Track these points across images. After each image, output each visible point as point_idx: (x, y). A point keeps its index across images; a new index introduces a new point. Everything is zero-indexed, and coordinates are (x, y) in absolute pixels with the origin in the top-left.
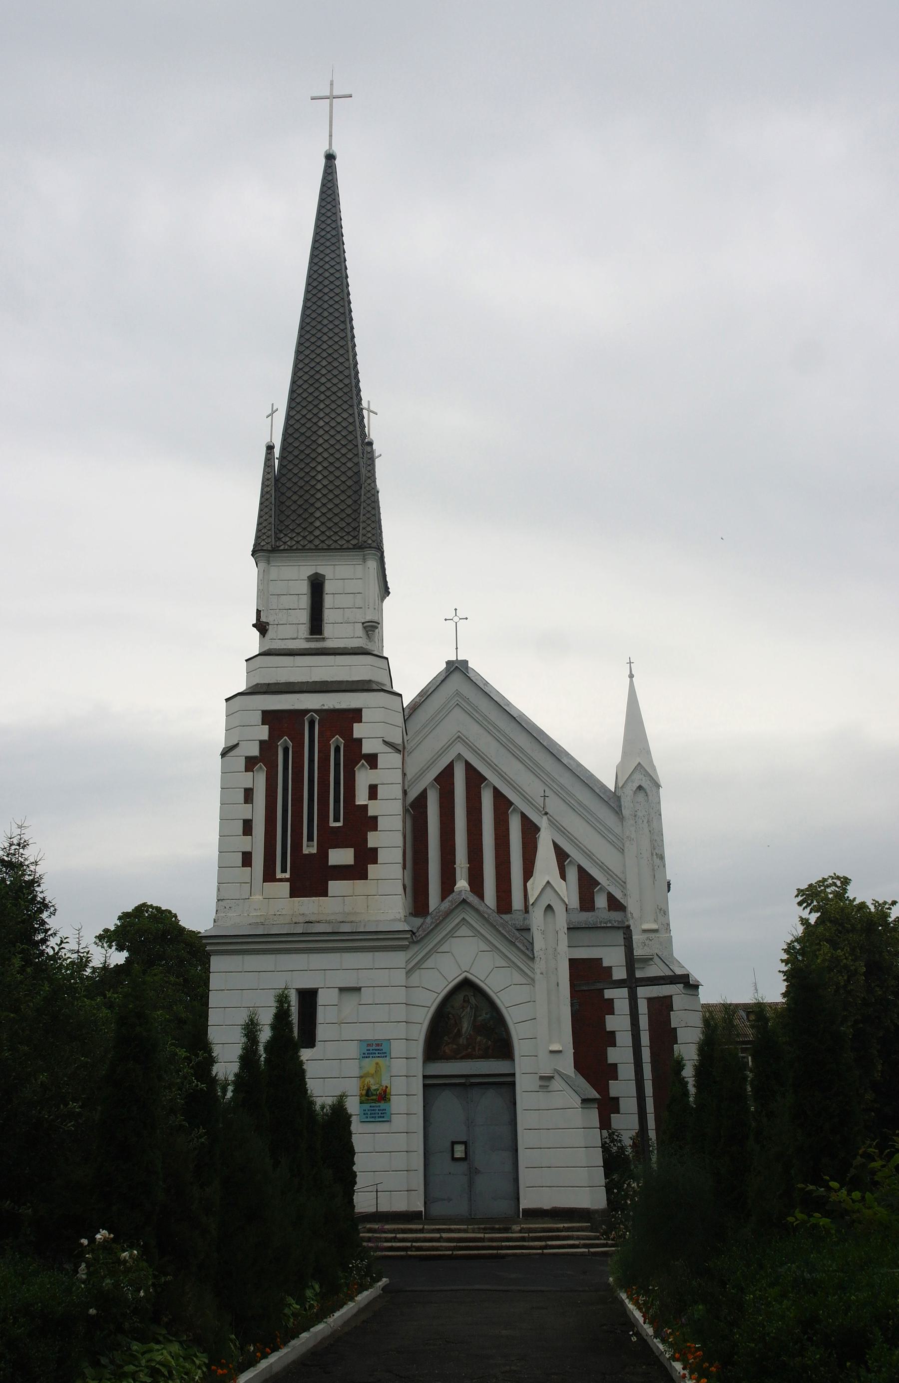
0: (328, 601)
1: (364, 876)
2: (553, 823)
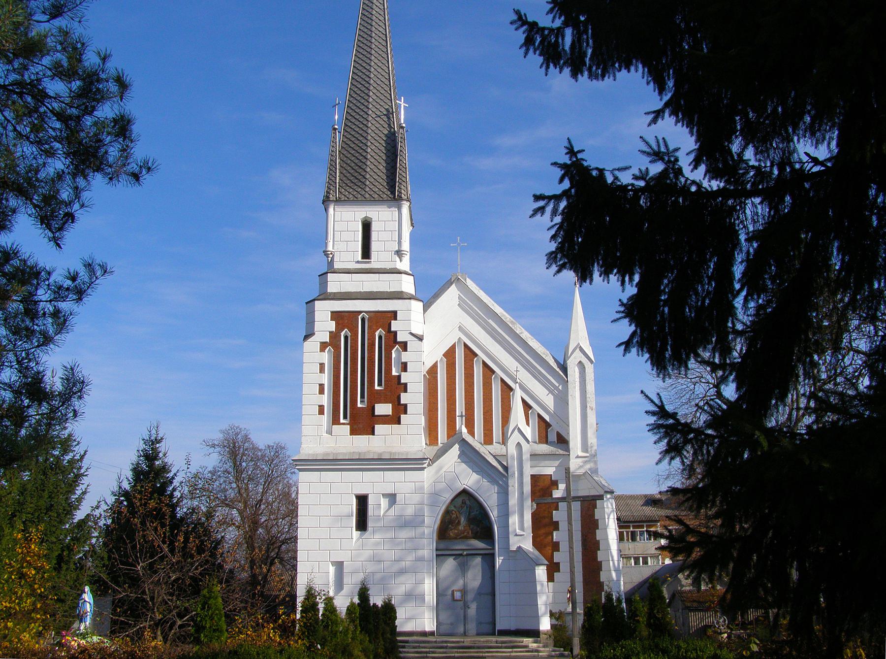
0: (374, 236)
1: (399, 423)
2: (522, 388)
